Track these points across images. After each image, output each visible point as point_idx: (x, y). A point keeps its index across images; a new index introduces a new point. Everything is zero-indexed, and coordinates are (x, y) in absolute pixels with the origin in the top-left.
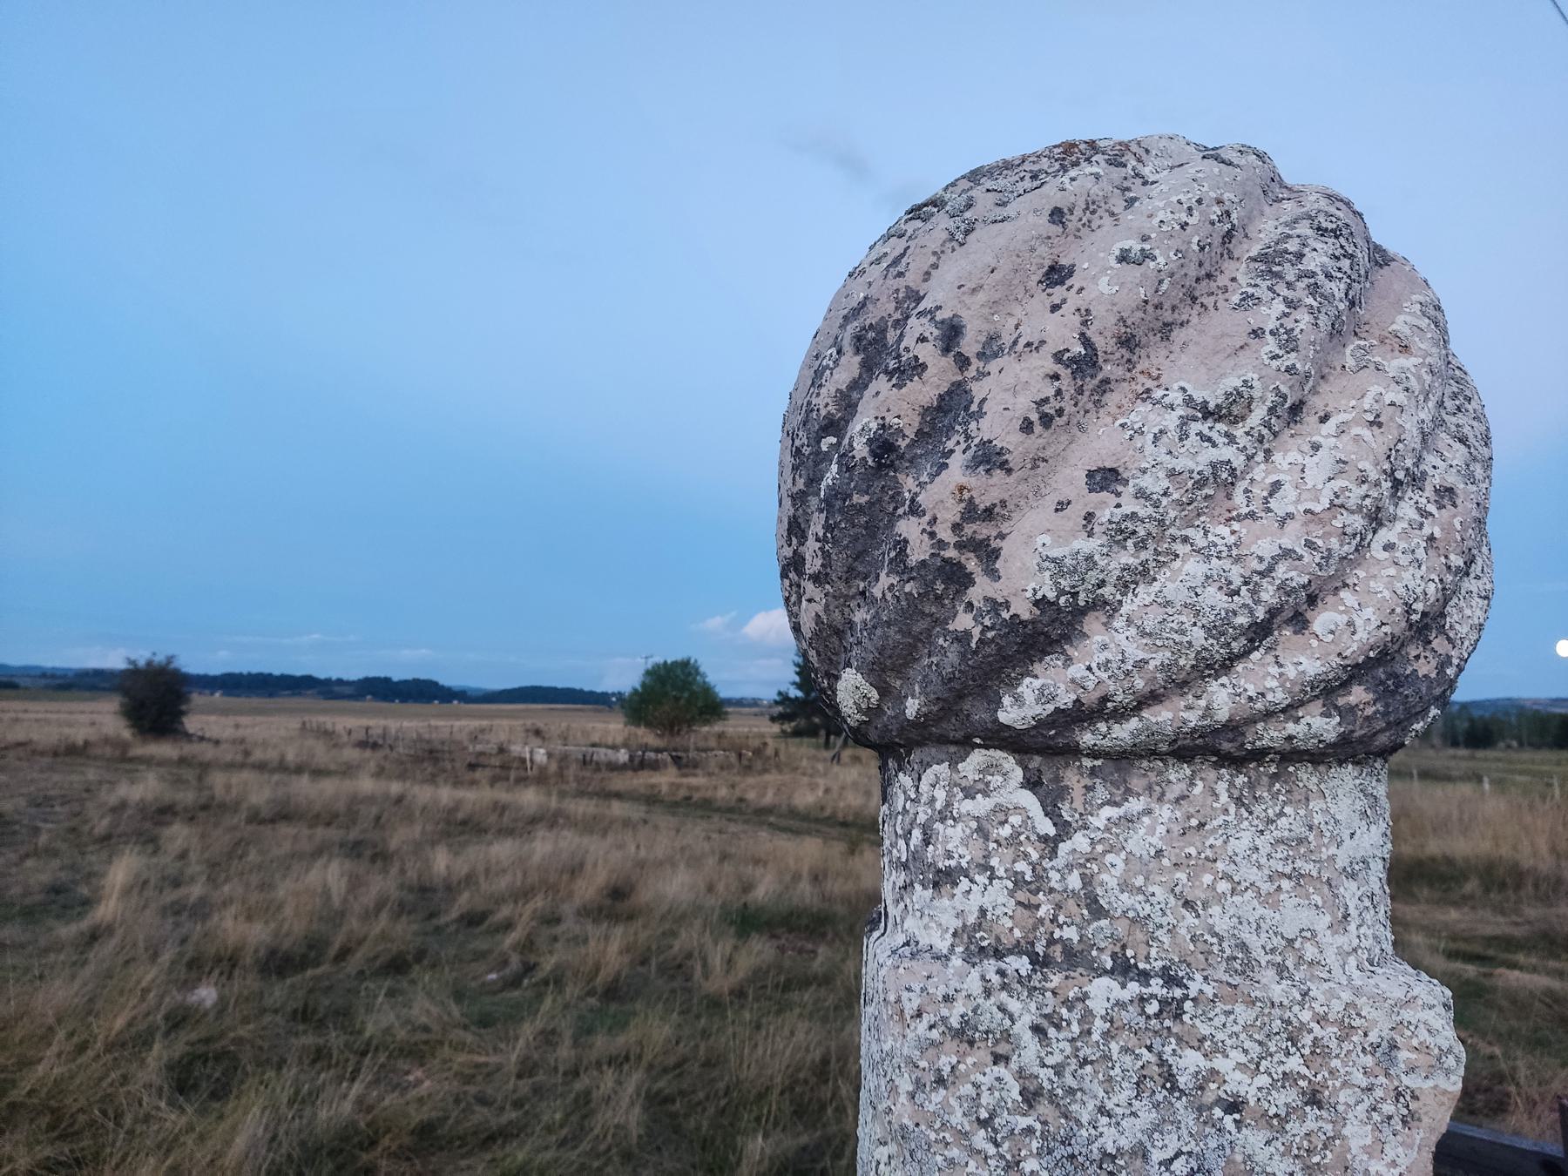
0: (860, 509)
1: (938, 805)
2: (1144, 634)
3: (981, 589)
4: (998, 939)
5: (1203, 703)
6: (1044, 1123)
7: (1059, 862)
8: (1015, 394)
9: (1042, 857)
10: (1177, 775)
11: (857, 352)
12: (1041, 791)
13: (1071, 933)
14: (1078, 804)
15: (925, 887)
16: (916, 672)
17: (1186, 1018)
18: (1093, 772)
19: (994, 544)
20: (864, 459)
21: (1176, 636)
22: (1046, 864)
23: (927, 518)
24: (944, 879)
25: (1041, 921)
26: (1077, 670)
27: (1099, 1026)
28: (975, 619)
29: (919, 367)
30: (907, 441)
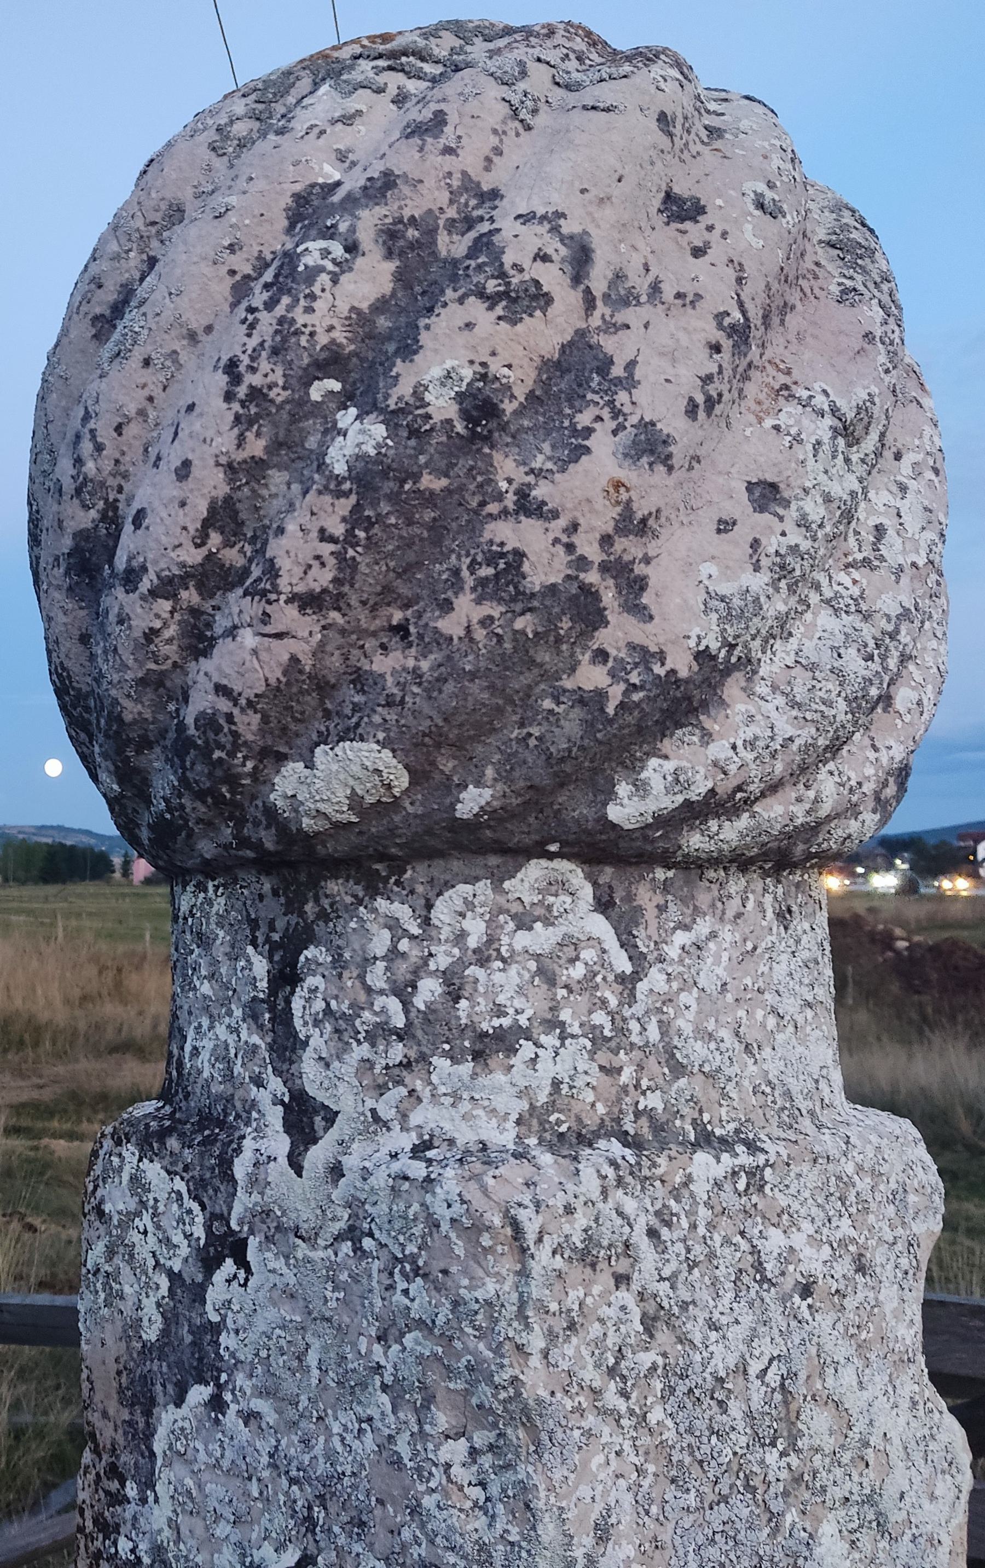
0: (429, 499)
1: (472, 942)
2: (794, 704)
3: (618, 632)
4: (579, 1120)
5: (811, 794)
6: (665, 1355)
7: (638, 1009)
8: (674, 361)
9: (621, 1004)
10: (736, 885)
11: (389, 255)
12: (614, 913)
13: (654, 1101)
14: (652, 930)
15: (455, 1061)
16: (489, 751)
17: (767, 1189)
18: (666, 887)
19: (639, 569)
20: (449, 421)
21: (823, 708)
22: (627, 1012)
23: (562, 522)
24: (489, 1046)
25: (625, 1089)
26: (719, 750)
27: (703, 1213)
28: (612, 674)
29: (539, 298)
30: (515, 404)
